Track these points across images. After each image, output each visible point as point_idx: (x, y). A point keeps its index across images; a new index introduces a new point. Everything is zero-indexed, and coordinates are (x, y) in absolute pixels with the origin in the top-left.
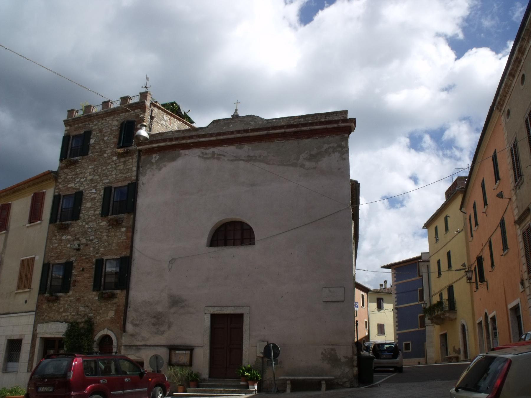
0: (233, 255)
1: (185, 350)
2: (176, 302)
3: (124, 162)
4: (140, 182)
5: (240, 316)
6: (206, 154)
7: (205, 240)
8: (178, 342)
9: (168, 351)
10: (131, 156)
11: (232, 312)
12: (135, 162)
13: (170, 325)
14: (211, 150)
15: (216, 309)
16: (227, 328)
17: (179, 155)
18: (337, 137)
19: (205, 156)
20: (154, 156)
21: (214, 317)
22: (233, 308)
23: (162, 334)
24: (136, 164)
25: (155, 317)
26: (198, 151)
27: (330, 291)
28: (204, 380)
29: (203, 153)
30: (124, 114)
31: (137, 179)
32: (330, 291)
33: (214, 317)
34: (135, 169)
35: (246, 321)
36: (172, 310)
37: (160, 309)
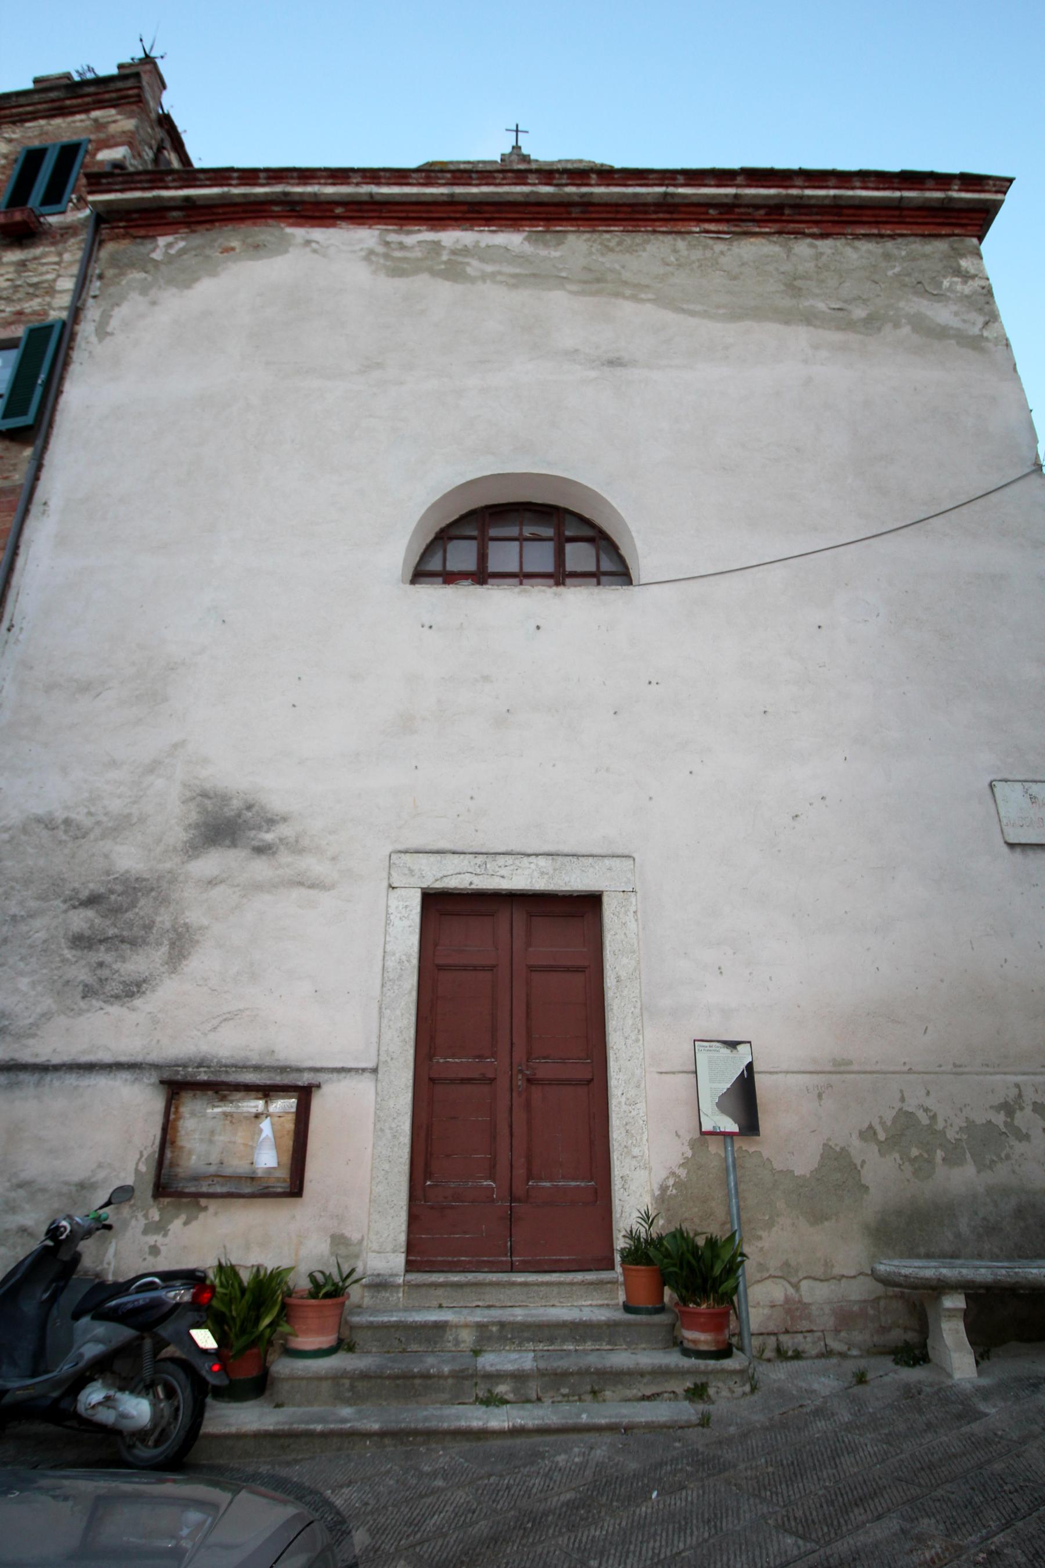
0: (527, 626)
1: (267, 1092)
2: (225, 825)
3: (22, 264)
4: (86, 329)
5: (590, 903)
6: (402, 246)
7: (397, 552)
8: (226, 1044)
9: (158, 1104)
10: (53, 244)
11: (540, 885)
12: (71, 264)
13: (181, 944)
14: (420, 237)
15: (453, 864)
17: (283, 247)
18: (941, 246)
19: (398, 254)
20: (162, 241)
21: (437, 904)
22: (542, 862)
23: (131, 995)
24: (75, 270)
25: (92, 901)
26: (366, 237)
27: (1033, 799)
28: (380, 1285)
29: (387, 244)
30: (42, 122)
31: (76, 312)
32: (1033, 799)
33: (437, 904)
34: (67, 284)
35: (618, 927)
36: (211, 863)
37: (128, 858)
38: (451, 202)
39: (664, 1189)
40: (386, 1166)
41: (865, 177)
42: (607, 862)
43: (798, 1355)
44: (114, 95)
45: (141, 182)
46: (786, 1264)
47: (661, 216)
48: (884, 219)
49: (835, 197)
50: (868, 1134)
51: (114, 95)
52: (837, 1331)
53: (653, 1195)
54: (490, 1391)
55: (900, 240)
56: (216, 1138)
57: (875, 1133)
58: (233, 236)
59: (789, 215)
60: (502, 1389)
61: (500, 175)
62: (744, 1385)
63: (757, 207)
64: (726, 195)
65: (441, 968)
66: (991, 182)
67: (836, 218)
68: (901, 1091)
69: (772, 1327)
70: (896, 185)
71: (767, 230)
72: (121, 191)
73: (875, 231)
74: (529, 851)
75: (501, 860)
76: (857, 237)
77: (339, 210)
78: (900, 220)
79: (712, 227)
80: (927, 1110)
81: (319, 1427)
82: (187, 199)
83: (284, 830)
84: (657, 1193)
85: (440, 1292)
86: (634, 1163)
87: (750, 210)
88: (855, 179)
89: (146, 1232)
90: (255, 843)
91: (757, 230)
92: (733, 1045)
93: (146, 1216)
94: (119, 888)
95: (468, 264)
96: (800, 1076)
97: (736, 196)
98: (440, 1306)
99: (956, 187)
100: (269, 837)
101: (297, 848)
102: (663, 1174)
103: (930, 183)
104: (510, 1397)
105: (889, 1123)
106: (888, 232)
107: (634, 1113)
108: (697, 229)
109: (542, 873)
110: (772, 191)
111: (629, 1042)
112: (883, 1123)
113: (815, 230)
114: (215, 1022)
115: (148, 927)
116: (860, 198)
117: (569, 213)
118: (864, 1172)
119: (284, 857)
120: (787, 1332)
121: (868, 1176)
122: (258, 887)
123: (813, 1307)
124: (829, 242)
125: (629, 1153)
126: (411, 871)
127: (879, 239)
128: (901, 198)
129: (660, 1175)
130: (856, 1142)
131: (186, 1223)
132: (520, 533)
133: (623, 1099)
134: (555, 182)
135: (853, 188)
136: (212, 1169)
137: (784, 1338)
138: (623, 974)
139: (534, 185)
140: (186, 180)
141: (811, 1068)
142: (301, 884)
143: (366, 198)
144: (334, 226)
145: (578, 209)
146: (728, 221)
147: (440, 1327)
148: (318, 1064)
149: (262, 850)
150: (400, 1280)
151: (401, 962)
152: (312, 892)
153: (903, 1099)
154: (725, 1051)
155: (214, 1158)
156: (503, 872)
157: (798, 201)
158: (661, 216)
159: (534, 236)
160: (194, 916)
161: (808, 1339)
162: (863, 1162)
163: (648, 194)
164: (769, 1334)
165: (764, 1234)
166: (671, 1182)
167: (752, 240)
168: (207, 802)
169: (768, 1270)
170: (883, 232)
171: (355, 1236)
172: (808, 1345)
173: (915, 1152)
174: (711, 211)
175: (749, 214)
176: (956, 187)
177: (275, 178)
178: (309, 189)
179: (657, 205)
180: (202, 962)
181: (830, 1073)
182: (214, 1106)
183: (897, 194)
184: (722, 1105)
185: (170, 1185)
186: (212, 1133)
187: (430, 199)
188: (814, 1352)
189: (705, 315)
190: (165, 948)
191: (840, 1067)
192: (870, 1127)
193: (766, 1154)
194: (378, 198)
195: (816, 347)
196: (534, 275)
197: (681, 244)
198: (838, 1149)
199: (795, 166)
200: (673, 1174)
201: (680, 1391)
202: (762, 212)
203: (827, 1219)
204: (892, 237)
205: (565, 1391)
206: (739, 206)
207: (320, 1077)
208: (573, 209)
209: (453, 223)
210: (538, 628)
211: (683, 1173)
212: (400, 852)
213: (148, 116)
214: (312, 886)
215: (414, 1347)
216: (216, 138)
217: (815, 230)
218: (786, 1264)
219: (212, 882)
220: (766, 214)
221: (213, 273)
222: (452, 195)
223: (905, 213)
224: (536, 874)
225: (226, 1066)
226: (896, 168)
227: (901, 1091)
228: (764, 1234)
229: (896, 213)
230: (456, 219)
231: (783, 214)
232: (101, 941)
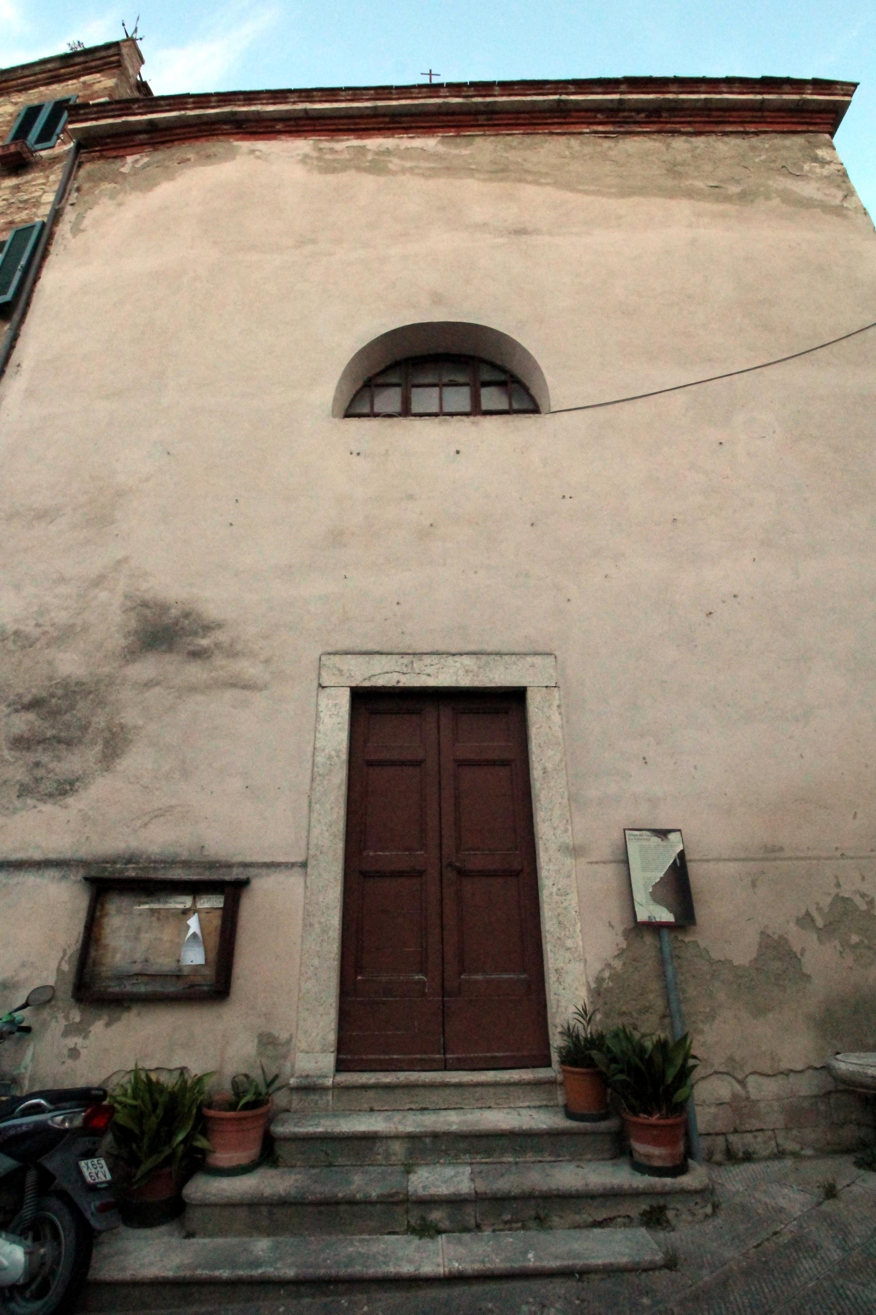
0: (447, 451)
1: (195, 888)
2: (164, 632)
3: (17, 188)
4: (64, 229)
5: (513, 699)
6: (333, 151)
7: (326, 391)
8: (156, 840)
9: (82, 902)
10: (41, 171)
11: (465, 682)
12: (55, 182)
13: (114, 744)
14: (346, 144)
16: (440, 764)
17: (231, 155)
18: (798, 141)
19: (329, 157)
20: (130, 159)
21: (366, 701)
22: (467, 661)
23: (64, 793)
24: (56, 187)
25: (35, 704)
26: (303, 145)
28: (309, 1088)
29: (320, 150)
30: (42, 89)
31: (56, 215)
33: (366, 701)
34: (50, 197)
35: (544, 721)
36: (146, 668)
37: (69, 664)
38: (375, 113)
39: (599, 980)
40: (316, 962)
41: (730, 82)
42: (529, 659)
43: (748, 1157)
44: (99, 62)
45: (113, 110)
46: (731, 1059)
47: (556, 120)
48: (749, 119)
49: (706, 100)
50: (806, 920)
51: (99, 62)
52: (787, 1129)
53: (589, 990)
54: (423, 1218)
55: (762, 136)
56: (143, 935)
57: (813, 920)
58: (188, 151)
59: (666, 117)
60: (436, 1215)
61: (416, 90)
62: (706, 1206)
63: (638, 111)
64: (612, 101)
65: (370, 764)
66: (839, 87)
67: (707, 119)
68: (836, 877)
69: (720, 1126)
70: (757, 90)
71: (648, 130)
72: (96, 119)
73: (741, 129)
74: (453, 651)
75: (427, 660)
76: (725, 134)
77: (279, 127)
78: (762, 120)
79: (600, 128)
80: (863, 895)
81: (225, 1274)
82: (151, 122)
83: (221, 636)
84: (593, 985)
85: (371, 1094)
86: (568, 955)
87: (633, 114)
88: (722, 85)
89: (66, 1033)
90: (191, 648)
91: (640, 129)
92: (663, 834)
93: (66, 1018)
94: (60, 692)
95: (390, 162)
96: (731, 864)
97: (620, 100)
98: (372, 1110)
99: (809, 91)
100: (204, 642)
101: (232, 653)
102: (598, 966)
103: (787, 88)
104: (446, 1224)
105: (826, 910)
106: (753, 130)
107: (566, 904)
108: (588, 130)
109: (467, 671)
110: (652, 96)
111: (558, 832)
112: (819, 909)
113: (690, 129)
114: (146, 819)
115: (84, 728)
116: (728, 100)
117: (477, 120)
118: (804, 960)
119: (219, 660)
120: (736, 1131)
121: (809, 964)
122: (193, 689)
123: (762, 1105)
124: (702, 139)
125: (563, 945)
126: (340, 671)
127: (744, 136)
128: (763, 100)
129: (596, 966)
130: (793, 928)
131: (108, 1025)
132: (441, 365)
133: (554, 889)
134: (463, 94)
135: (721, 93)
136: (137, 968)
137: (733, 1138)
138: (549, 766)
139: (446, 97)
140: (149, 106)
141: (742, 855)
142: (234, 685)
143: (301, 114)
144: (275, 139)
145: (484, 117)
146: (613, 123)
147: (370, 1138)
148: (248, 859)
149: (197, 655)
150: (329, 1082)
151: (330, 757)
152: (247, 693)
153: (838, 885)
154: (655, 840)
155: (139, 956)
156: (429, 670)
157: (673, 105)
158: (556, 120)
159: (446, 140)
160: (130, 717)
161: (759, 1139)
162: (803, 950)
163: (544, 101)
164: (717, 1134)
165: (706, 1028)
166: (607, 974)
167: (635, 138)
168: (148, 612)
169: (712, 1065)
170: (748, 129)
171: (284, 1036)
172: (758, 1144)
173: (855, 939)
174: (599, 115)
175: (632, 117)
176: (809, 91)
177: (224, 101)
178: (253, 108)
179: (551, 111)
180: (136, 760)
181: (762, 859)
182: (140, 903)
183: (759, 97)
184: (656, 896)
185: (93, 988)
186: (139, 930)
187: (355, 113)
188: (765, 1153)
189: (598, 193)
190: (99, 748)
191: (772, 852)
192: (808, 914)
193: (702, 944)
194: (311, 114)
195: (699, 215)
196: (448, 169)
197: (574, 142)
198: (776, 937)
199: (670, 74)
200: (609, 966)
201: (635, 1213)
202: (643, 115)
203: (769, 1010)
204: (757, 133)
205: (508, 1217)
206: (624, 110)
207: (252, 872)
208: (479, 117)
209: (376, 132)
210: (458, 452)
211: (618, 964)
212: (329, 654)
213: (128, 81)
214: (245, 687)
215: (341, 1161)
216: (172, 71)
217: (689, 129)
218: (731, 1059)
219: (149, 685)
220: (646, 117)
221: (171, 177)
222: (376, 108)
223: (766, 114)
224: (461, 672)
225: (155, 862)
226: (757, 75)
227: (836, 877)
228: (706, 1028)
229: (759, 114)
230: (379, 129)
231: (660, 117)
232: (39, 742)
